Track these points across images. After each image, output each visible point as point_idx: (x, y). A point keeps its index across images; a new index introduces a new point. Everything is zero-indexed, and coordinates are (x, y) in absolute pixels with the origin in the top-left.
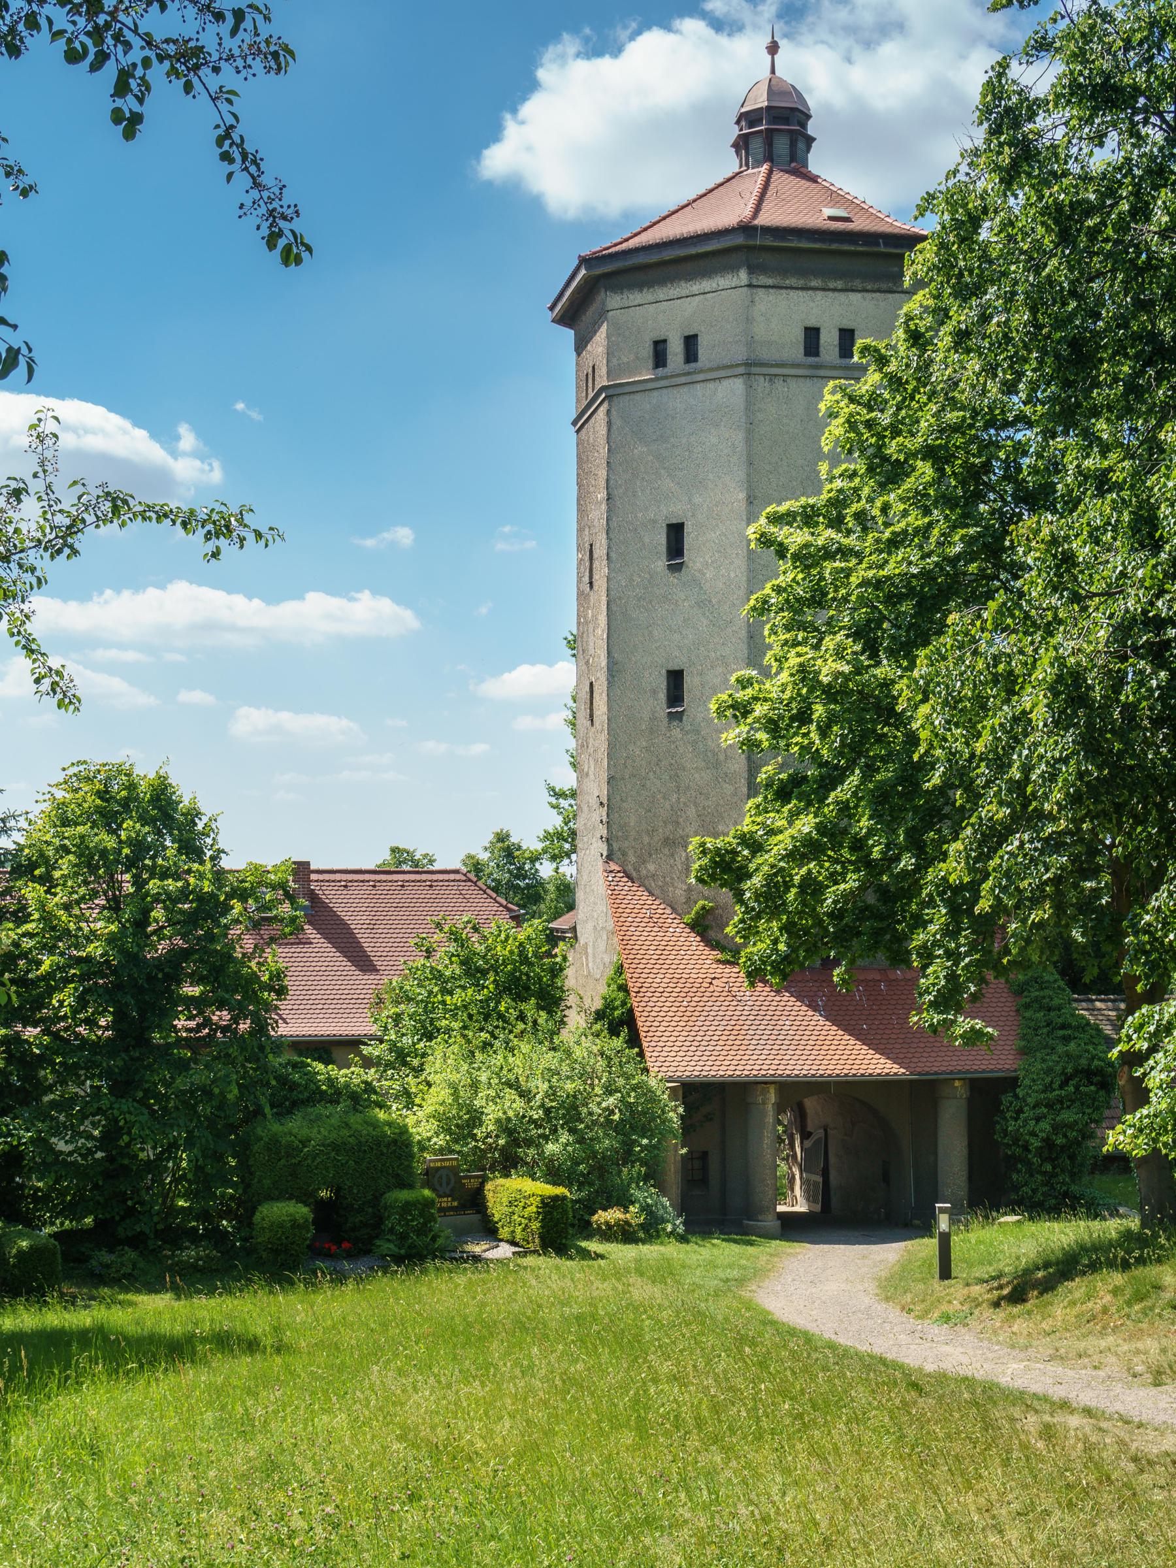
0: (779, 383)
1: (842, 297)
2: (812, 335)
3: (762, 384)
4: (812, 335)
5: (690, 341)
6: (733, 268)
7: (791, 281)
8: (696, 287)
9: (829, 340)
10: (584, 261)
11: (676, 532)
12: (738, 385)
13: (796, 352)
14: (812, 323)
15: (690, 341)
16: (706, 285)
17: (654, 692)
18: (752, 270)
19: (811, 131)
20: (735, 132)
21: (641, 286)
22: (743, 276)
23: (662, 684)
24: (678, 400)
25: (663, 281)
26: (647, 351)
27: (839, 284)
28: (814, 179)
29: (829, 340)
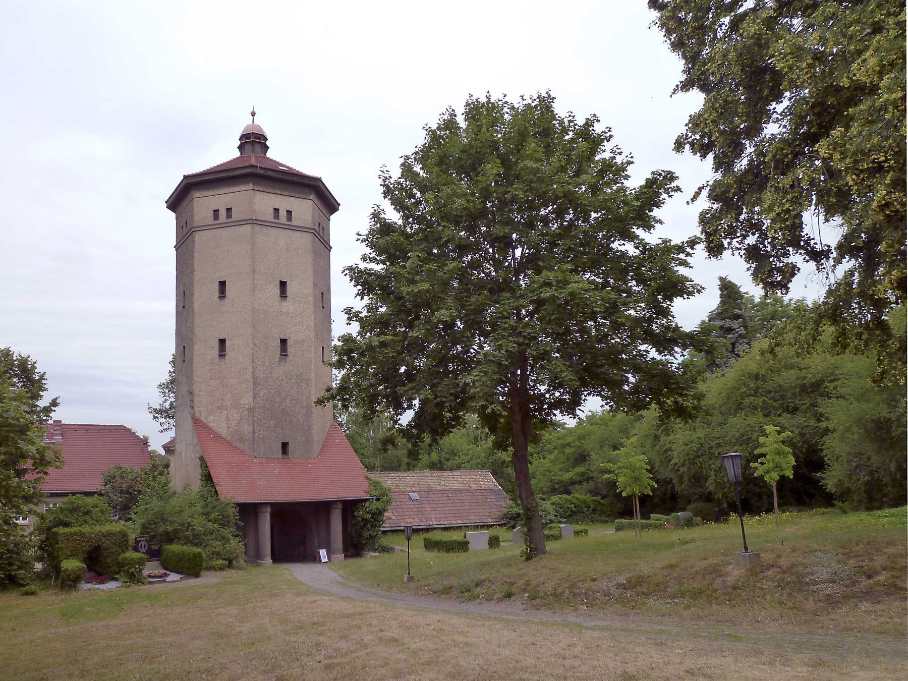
0: (264, 228)
1: (287, 198)
2: (277, 210)
3: (258, 228)
4: (277, 210)
5: (229, 210)
6: (247, 183)
7: (269, 190)
8: (231, 190)
9: (283, 213)
10: (185, 177)
11: (223, 284)
12: (248, 227)
13: (270, 218)
14: (277, 207)
15: (229, 210)
16: (236, 189)
17: (213, 347)
18: (254, 184)
19: (268, 143)
20: (239, 143)
21: (208, 189)
22: (251, 186)
23: (217, 344)
24: (224, 233)
25: (217, 187)
26: (211, 214)
27: (286, 193)
28: (271, 160)
29: (283, 213)
